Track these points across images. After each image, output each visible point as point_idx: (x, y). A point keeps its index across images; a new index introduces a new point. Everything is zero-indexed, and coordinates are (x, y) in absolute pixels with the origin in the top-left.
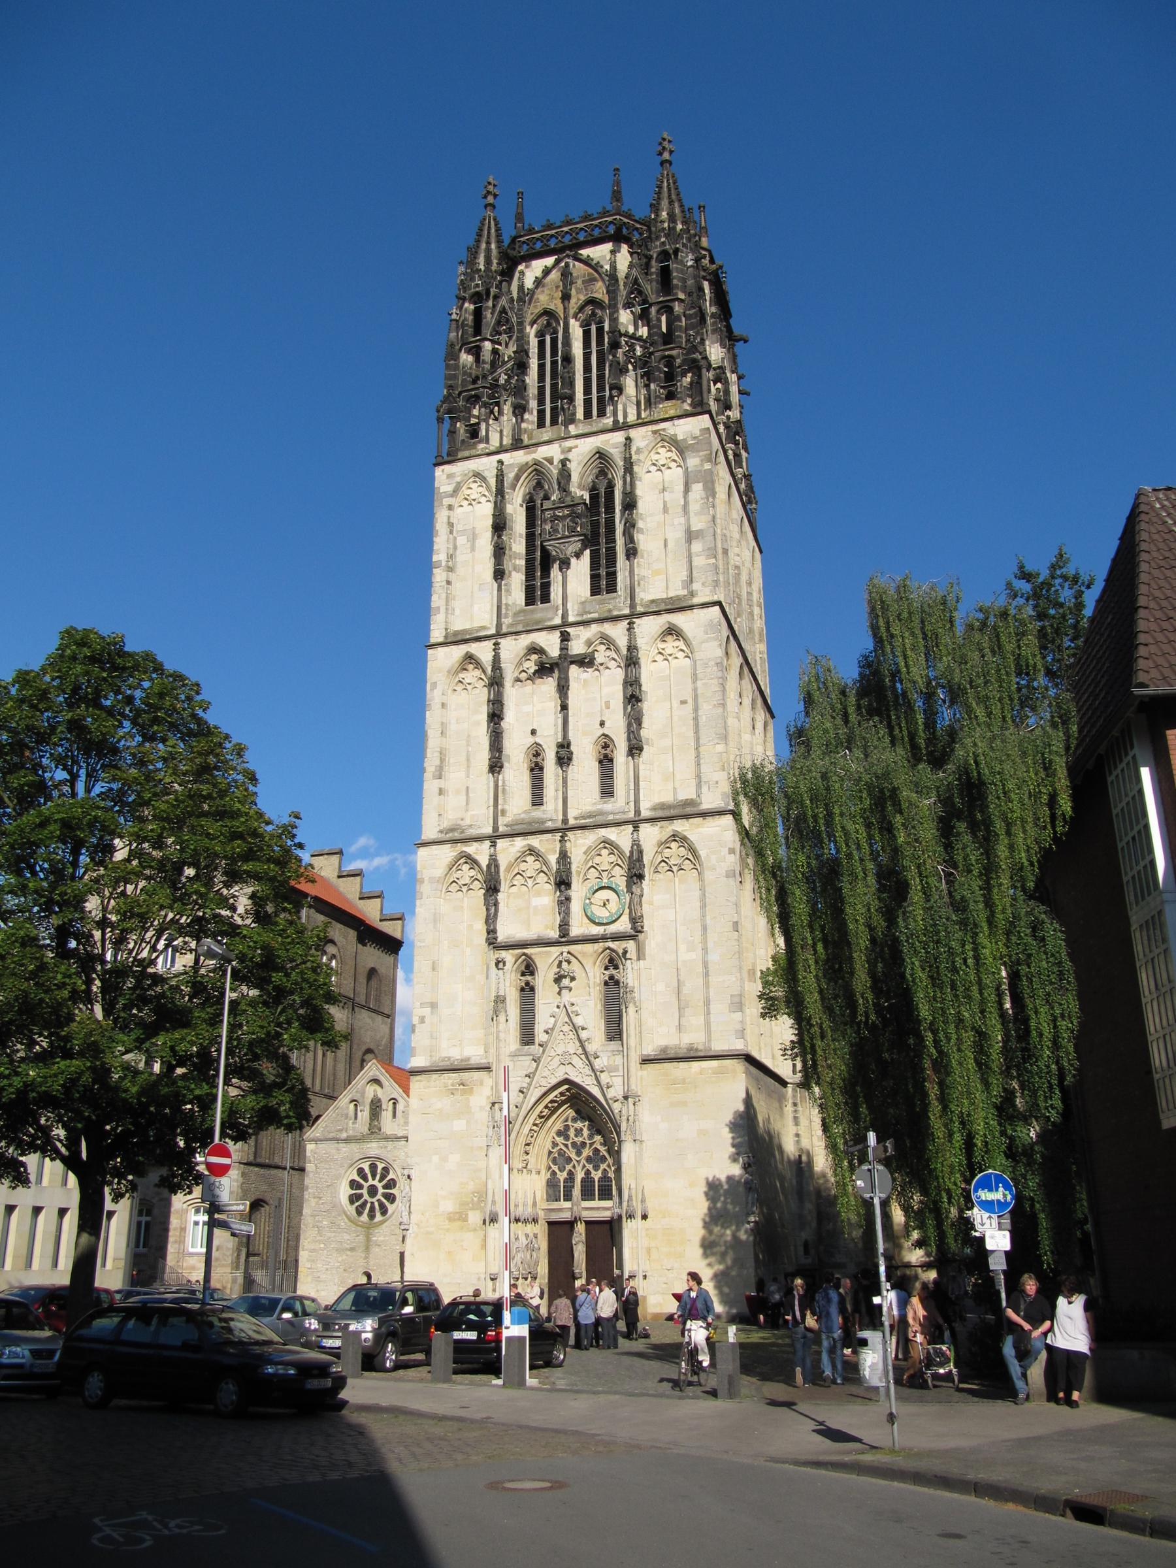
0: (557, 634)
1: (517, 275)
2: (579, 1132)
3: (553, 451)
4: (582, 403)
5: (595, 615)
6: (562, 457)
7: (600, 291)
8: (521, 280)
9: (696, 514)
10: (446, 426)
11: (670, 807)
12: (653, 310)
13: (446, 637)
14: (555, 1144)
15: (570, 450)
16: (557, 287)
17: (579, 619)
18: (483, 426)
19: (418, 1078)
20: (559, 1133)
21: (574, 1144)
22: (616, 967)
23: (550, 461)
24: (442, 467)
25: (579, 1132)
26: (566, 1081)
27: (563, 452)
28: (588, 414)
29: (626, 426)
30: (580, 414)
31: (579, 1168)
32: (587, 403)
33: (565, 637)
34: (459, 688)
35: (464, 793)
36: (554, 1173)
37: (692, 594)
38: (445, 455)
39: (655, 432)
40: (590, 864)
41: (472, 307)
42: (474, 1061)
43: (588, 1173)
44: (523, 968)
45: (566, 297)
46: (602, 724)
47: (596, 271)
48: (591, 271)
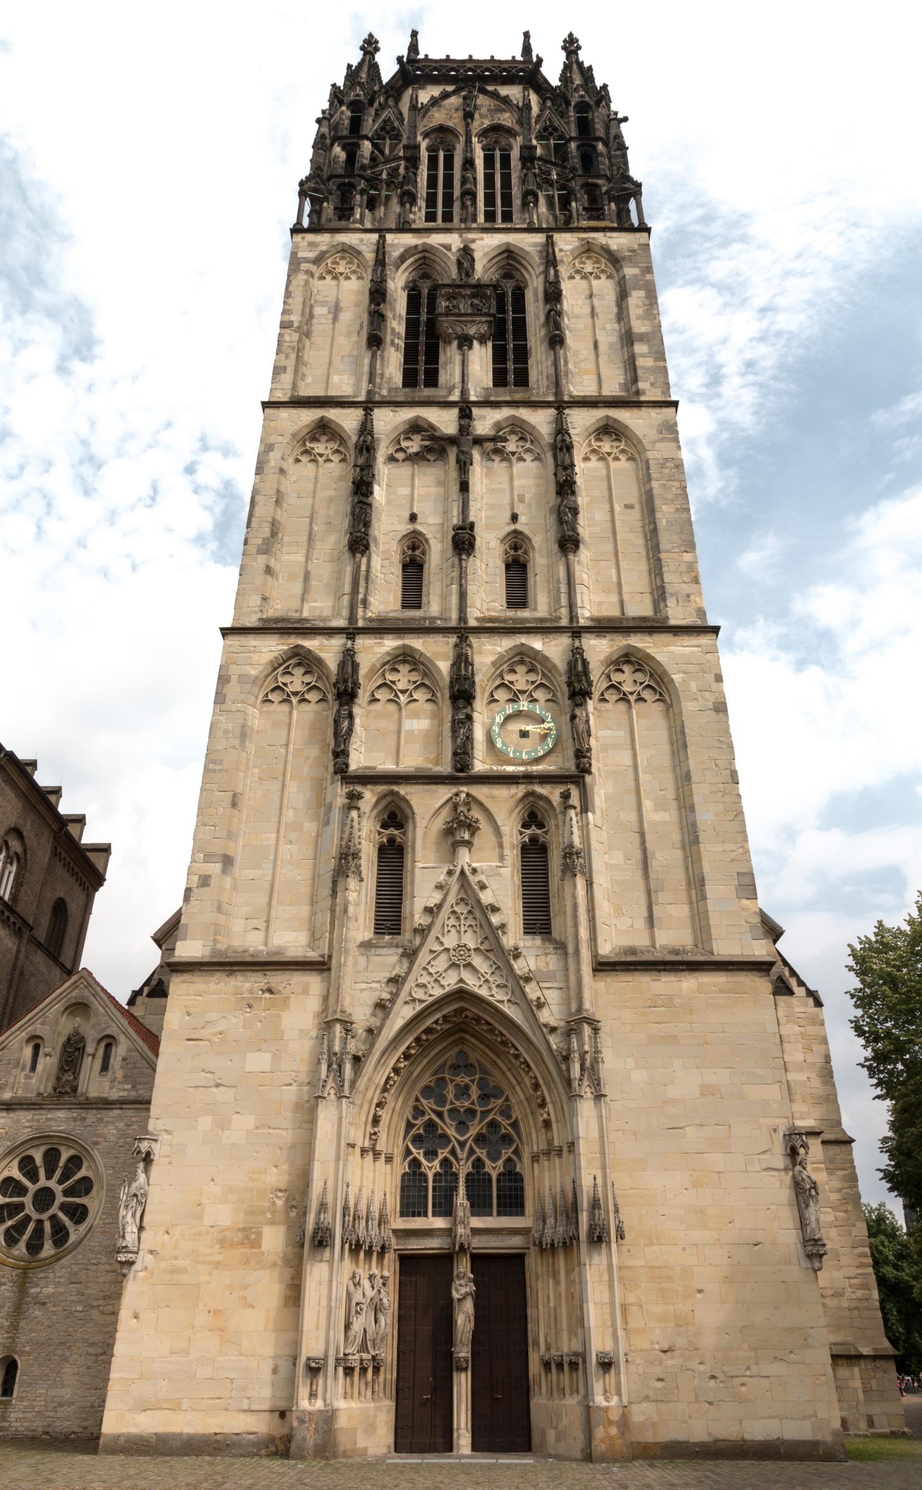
0: (455, 412)
7: (507, 119)
22: (541, 826)
26: (461, 994)
34: (305, 459)
38: (306, 223)
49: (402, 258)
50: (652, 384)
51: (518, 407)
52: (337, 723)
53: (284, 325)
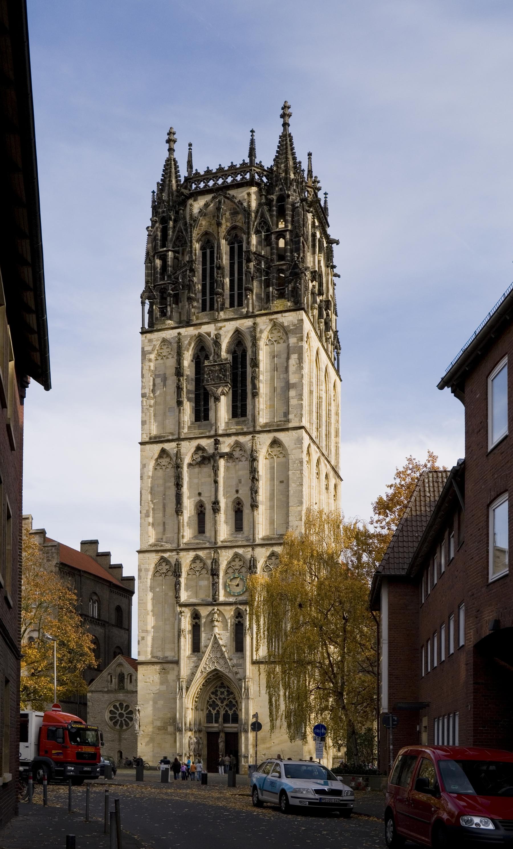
0: (212, 440)
1: (188, 206)
2: (222, 693)
3: (210, 329)
4: (228, 297)
5: (234, 431)
6: (216, 333)
8: (191, 210)
9: (293, 374)
10: (147, 307)
11: (271, 539)
12: (273, 237)
13: (150, 438)
14: (210, 698)
15: (220, 328)
16: (214, 216)
17: (225, 432)
18: (169, 309)
19: (142, 666)
20: (213, 693)
21: (220, 698)
23: (209, 334)
24: (145, 335)
25: (222, 693)
27: (216, 330)
28: (232, 305)
29: (255, 316)
30: (227, 304)
31: (222, 709)
32: (232, 296)
33: (217, 442)
35: (162, 525)
36: (210, 711)
37: (288, 421)
38: (146, 326)
39: (271, 320)
40: (229, 566)
41: (161, 226)
42: (170, 658)
43: (226, 711)
44: (194, 616)
45: (219, 224)
46: (237, 491)
47: (238, 207)
48: (235, 206)
49: (190, 344)
50: (295, 416)
51: (238, 435)
52: (176, 586)
53: (143, 395)
